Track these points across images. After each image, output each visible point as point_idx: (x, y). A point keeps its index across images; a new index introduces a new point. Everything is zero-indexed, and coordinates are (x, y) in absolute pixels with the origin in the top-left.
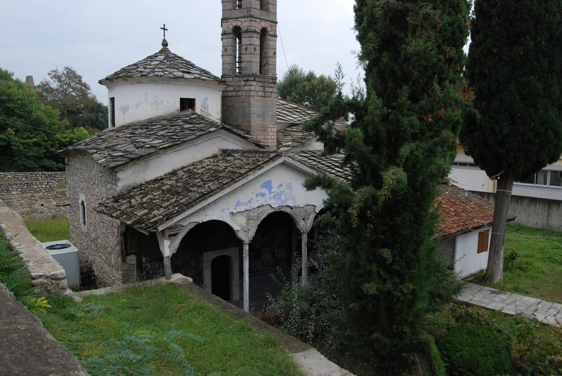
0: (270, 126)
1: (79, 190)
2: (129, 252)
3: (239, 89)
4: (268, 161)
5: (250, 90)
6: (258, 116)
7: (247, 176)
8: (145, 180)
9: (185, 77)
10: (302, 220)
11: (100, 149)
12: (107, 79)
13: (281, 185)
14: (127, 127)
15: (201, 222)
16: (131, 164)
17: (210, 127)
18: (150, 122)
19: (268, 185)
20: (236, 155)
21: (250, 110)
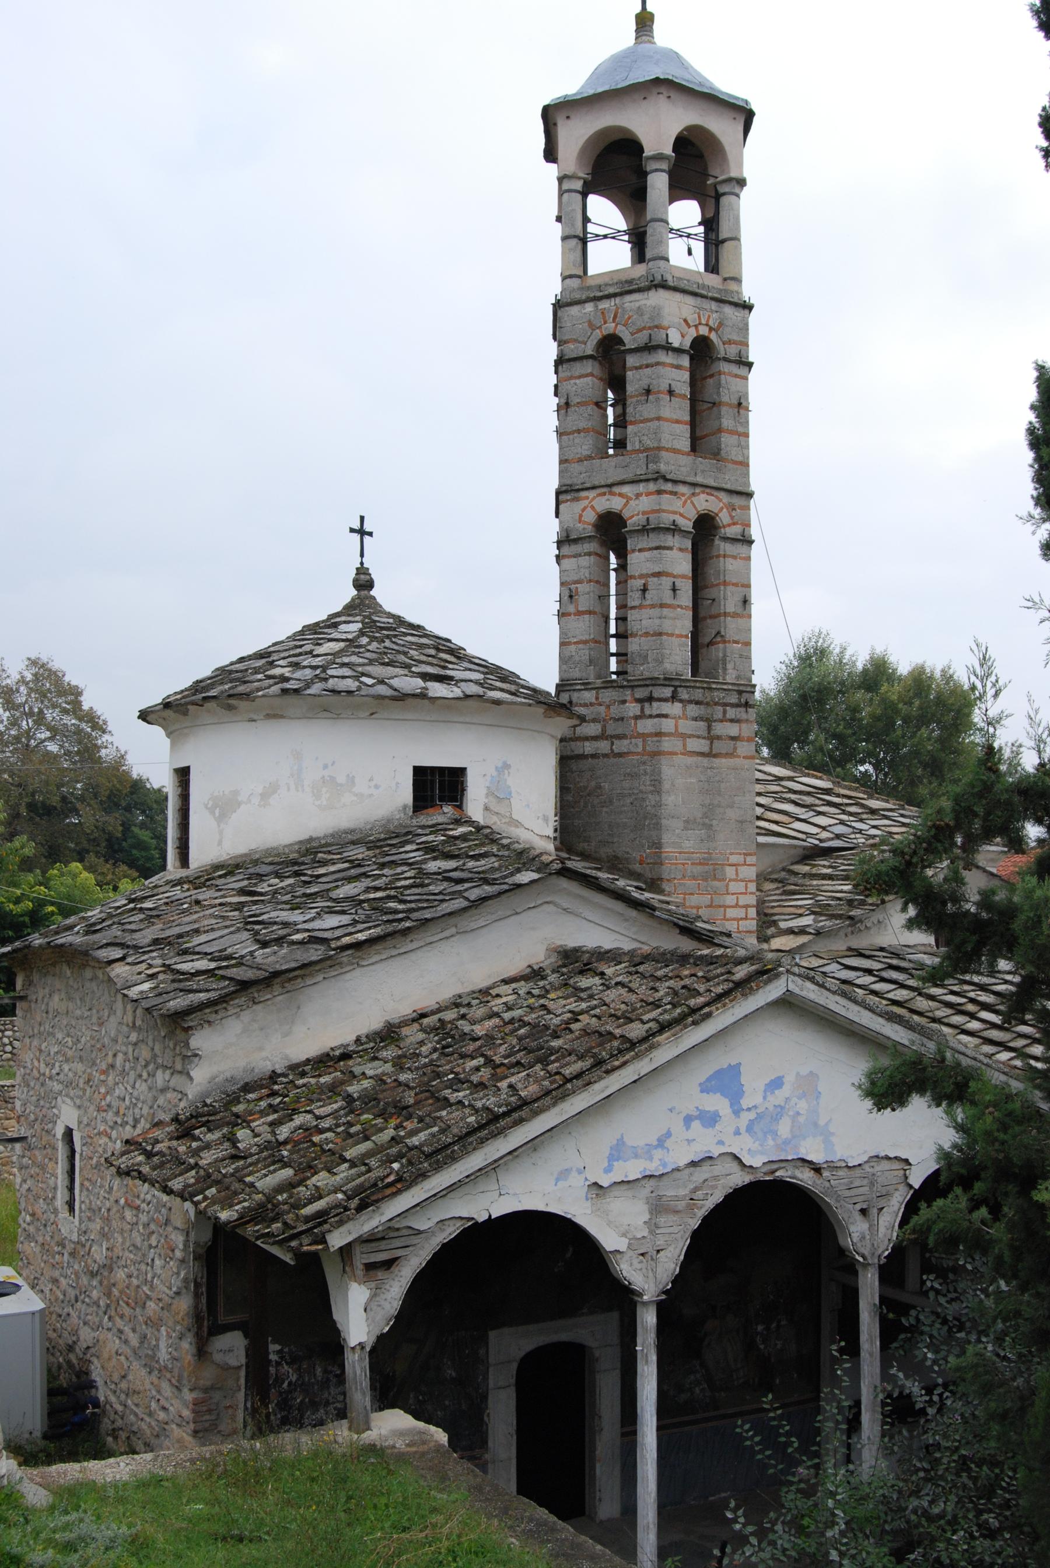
0: (733, 859)
1: (57, 1087)
2: (222, 1319)
3: (619, 731)
4: (726, 994)
5: (659, 734)
6: (688, 824)
7: (652, 1047)
8: (287, 1057)
9: (431, 694)
10: (858, 1216)
11: (136, 947)
12: (167, 705)
13: (777, 1083)
14: (230, 868)
15: (482, 1217)
16: (241, 1000)
17: (518, 870)
18: (307, 852)
19: (727, 1082)
20: (609, 971)
21: (659, 805)
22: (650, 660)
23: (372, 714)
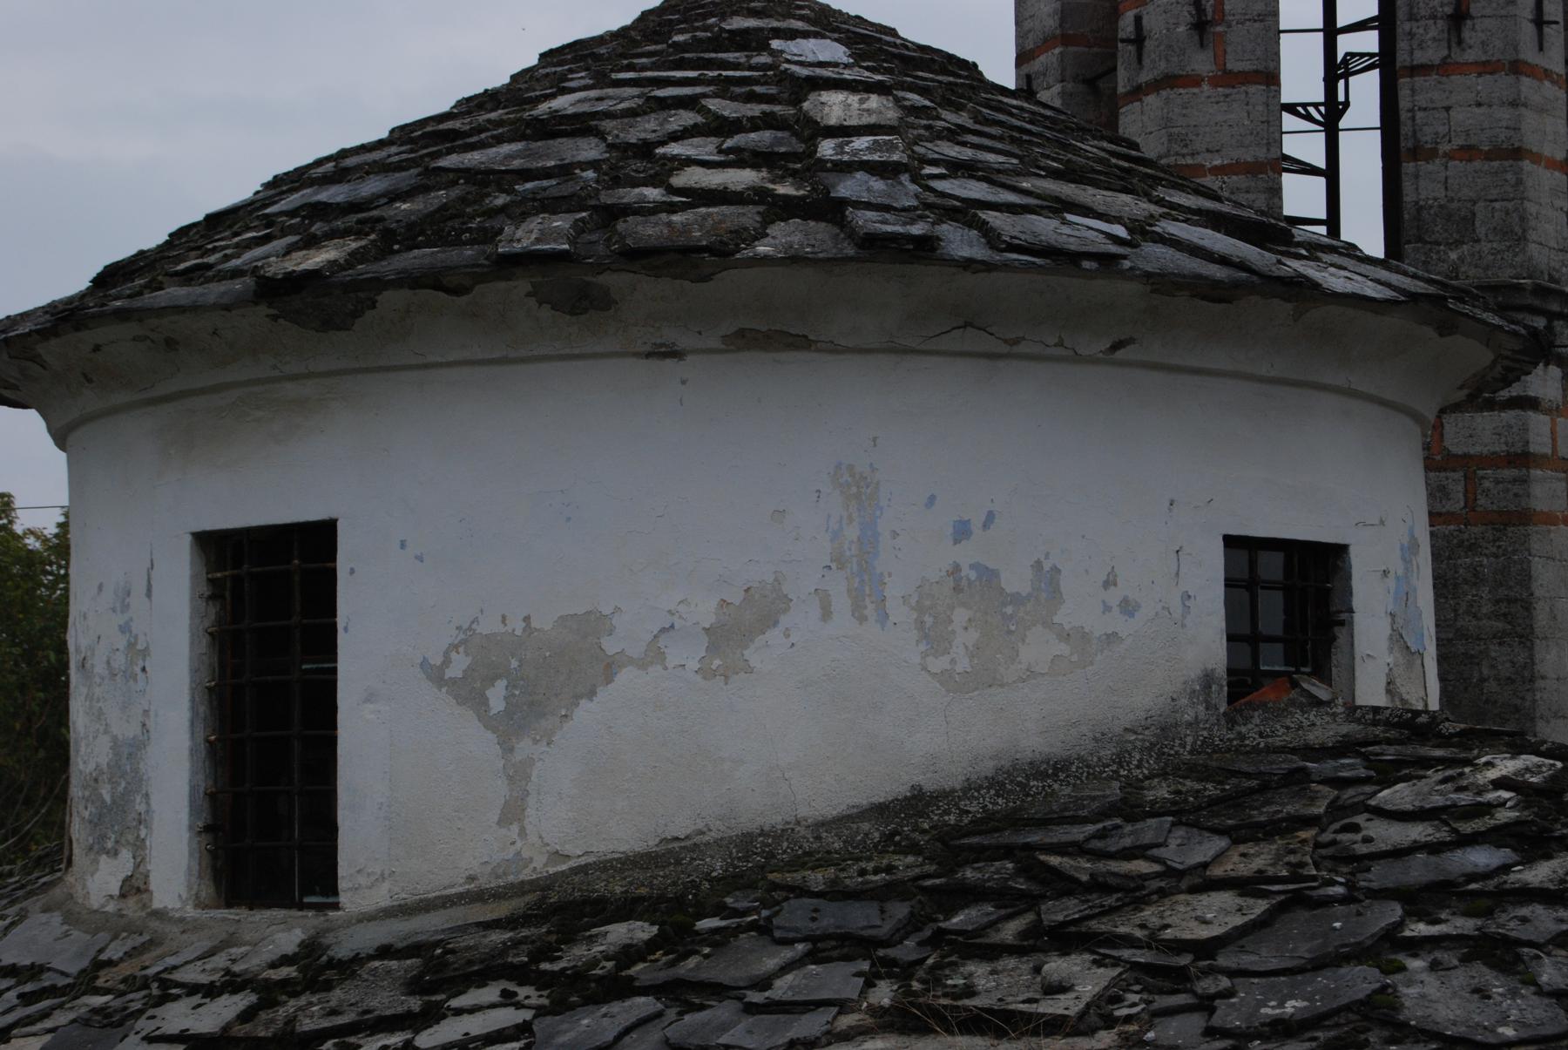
5: (1522, 459)
21: (1526, 676)
22: (1481, 231)
23: (1116, 347)
